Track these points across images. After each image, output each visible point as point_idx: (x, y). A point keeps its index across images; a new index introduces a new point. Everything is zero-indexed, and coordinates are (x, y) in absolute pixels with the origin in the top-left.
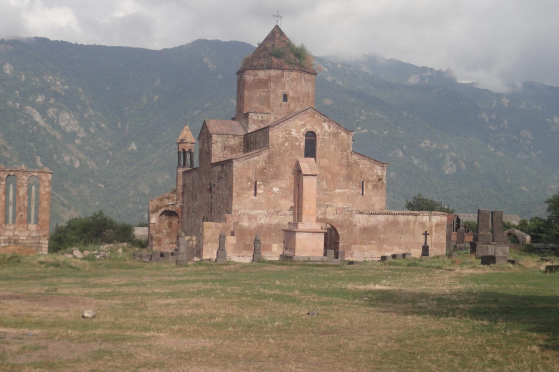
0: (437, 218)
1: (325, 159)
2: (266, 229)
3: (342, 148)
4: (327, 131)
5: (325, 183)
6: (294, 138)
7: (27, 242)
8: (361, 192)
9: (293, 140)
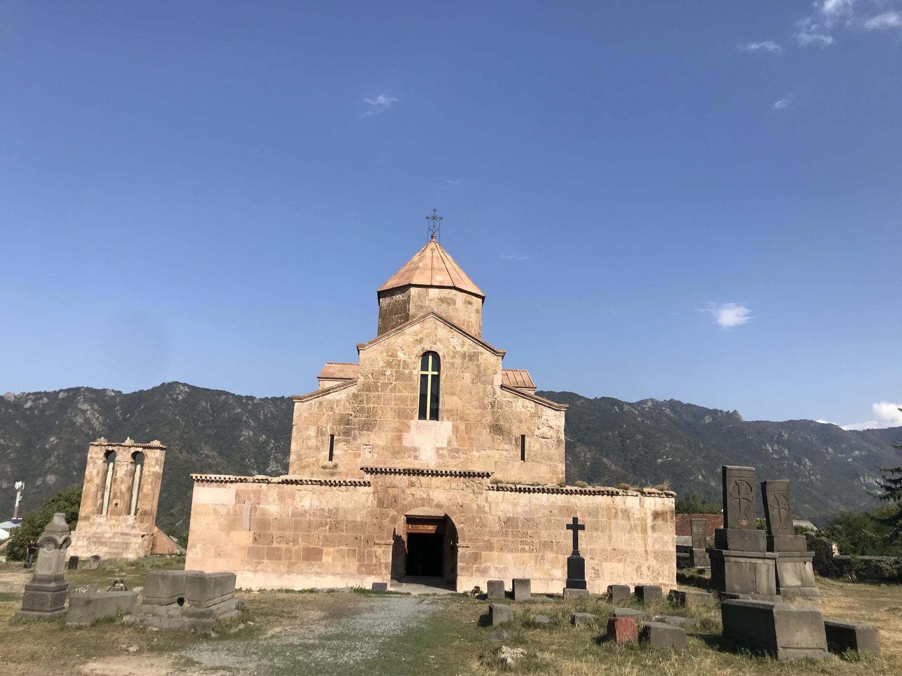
6: (402, 362)
9: (399, 365)
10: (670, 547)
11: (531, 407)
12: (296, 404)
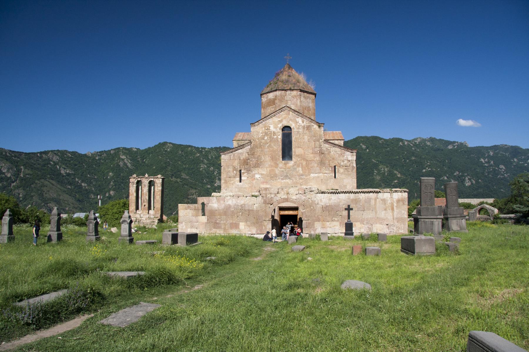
0: (398, 194)
1: (300, 149)
2: (233, 209)
3: (314, 138)
4: (301, 126)
5: (300, 169)
6: (272, 132)
7: (146, 221)
8: (334, 176)
9: (271, 134)
10: (405, 216)
11: (339, 152)
12: (222, 156)
